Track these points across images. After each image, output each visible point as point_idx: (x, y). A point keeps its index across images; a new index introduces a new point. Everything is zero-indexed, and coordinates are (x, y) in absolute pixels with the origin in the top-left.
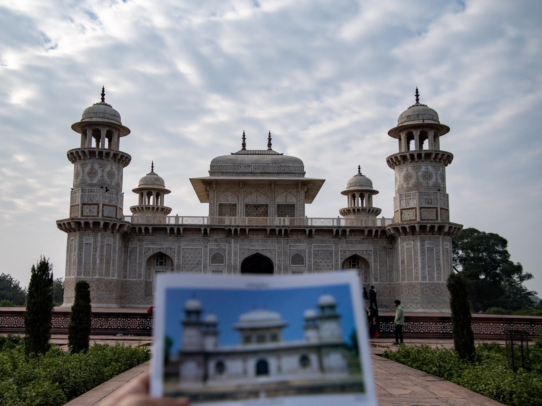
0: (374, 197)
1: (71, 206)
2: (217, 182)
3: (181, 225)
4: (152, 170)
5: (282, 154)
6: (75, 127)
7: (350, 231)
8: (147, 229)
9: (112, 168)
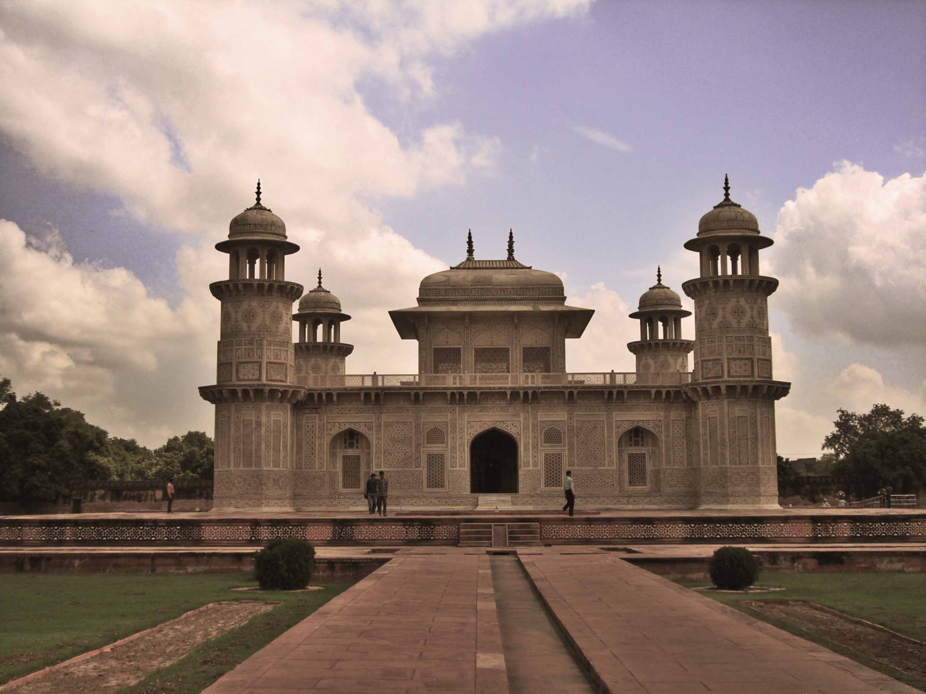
0: (683, 320)
1: (220, 365)
2: (431, 316)
3: (380, 388)
4: (320, 283)
5: (530, 268)
6: (221, 247)
7: (629, 392)
8: (329, 395)
9: (277, 307)
